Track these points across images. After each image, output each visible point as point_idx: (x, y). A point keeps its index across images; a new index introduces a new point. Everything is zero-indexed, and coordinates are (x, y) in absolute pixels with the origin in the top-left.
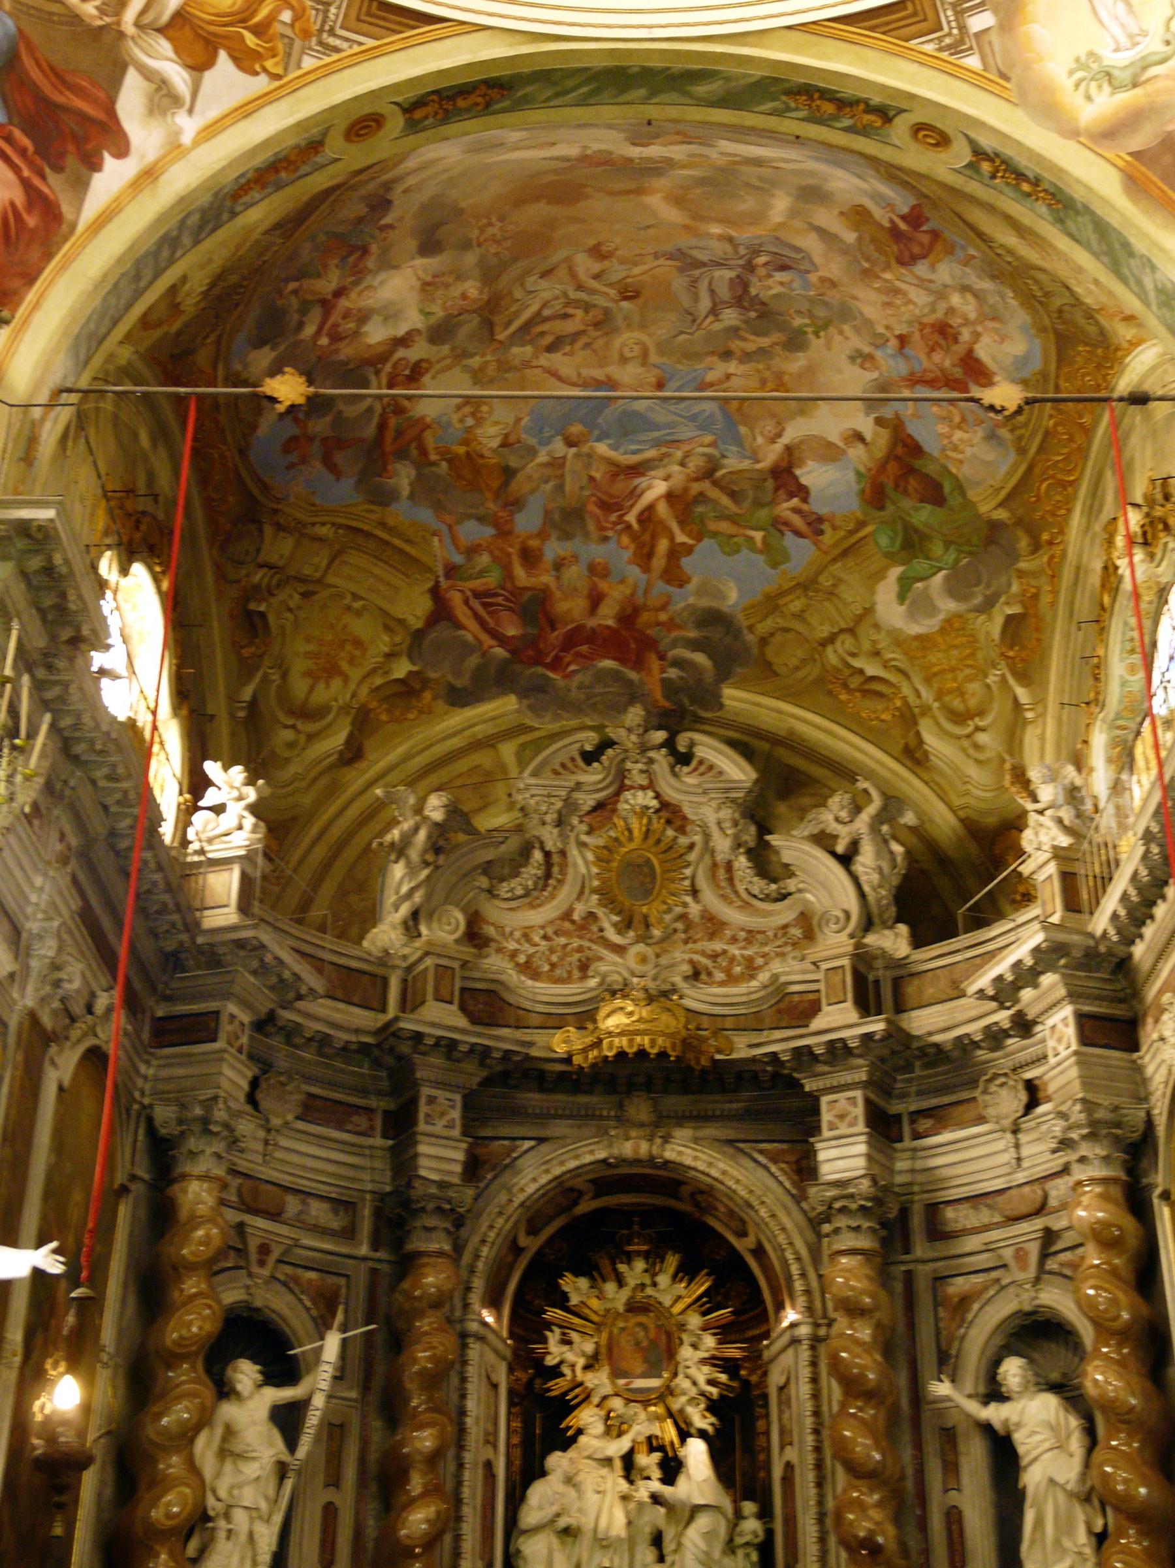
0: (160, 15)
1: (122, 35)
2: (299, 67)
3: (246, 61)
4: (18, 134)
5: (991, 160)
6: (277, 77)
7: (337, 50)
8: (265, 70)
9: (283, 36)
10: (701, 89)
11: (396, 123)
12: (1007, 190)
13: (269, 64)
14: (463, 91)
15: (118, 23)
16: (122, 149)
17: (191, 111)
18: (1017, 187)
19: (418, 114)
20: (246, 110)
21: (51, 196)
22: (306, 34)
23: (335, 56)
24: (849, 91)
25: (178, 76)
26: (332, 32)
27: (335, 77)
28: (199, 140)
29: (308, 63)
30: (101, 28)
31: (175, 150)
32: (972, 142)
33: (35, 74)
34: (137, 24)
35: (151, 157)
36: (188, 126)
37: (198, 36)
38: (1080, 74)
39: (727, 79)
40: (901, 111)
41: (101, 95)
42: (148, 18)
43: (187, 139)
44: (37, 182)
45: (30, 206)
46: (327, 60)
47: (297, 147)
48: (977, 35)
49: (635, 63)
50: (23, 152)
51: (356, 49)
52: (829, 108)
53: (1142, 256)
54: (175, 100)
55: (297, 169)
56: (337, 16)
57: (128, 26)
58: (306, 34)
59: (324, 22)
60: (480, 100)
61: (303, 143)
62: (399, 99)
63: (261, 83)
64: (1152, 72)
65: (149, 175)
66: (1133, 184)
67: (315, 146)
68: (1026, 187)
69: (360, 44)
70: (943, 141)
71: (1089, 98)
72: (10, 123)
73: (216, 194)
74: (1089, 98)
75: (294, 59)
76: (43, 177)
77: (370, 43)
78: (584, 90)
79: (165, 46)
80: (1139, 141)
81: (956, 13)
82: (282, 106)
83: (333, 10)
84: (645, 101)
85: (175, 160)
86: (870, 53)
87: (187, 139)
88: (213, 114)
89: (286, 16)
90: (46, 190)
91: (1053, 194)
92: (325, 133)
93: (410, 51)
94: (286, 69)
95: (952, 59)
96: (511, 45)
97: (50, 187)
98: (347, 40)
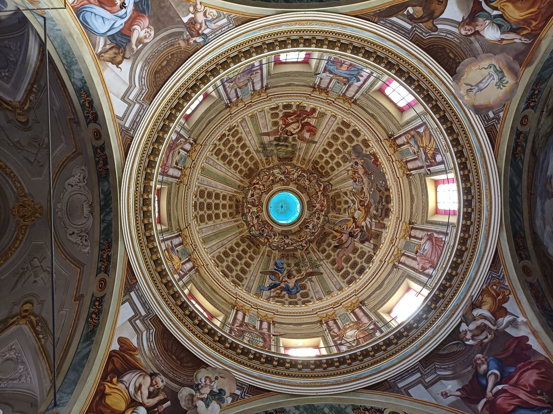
0: (493, 319)
1: (497, 330)
2: (508, 286)
3: (505, 300)
4: (519, 366)
5: (530, 103)
6: (510, 292)
7: (504, 276)
8: (508, 295)
9: (499, 289)
10: (516, 182)
11: (526, 262)
12: (539, 97)
13: (507, 294)
14: (516, 244)
15: (494, 330)
16: (526, 338)
17: (518, 317)
18: (537, 94)
19: (524, 256)
20: (519, 303)
21: (537, 362)
22: (499, 283)
23: (505, 276)
24: (513, 144)
25: (508, 318)
26: (499, 276)
27: (511, 277)
28: (526, 317)
29: (507, 284)
30: (494, 335)
31: (528, 324)
32: (524, 110)
33: (504, 356)
34: (494, 326)
35: (529, 331)
36: (521, 319)
37: (498, 311)
38: (501, 86)
39: (512, 176)
40: (517, 130)
41: (511, 340)
42: (493, 323)
43: (525, 320)
44: (533, 364)
45: (540, 369)
46: (506, 279)
47: (531, 290)
48: (494, 114)
49: (508, 199)
50: (524, 366)
51: (503, 271)
52: (519, 149)
53: (550, 54)
54: (514, 320)
55: (539, 291)
56: (495, 274)
57: (495, 328)
58: (499, 283)
59: (497, 278)
60: (520, 240)
61: (530, 288)
62: (518, 261)
63: (511, 296)
64: (498, 68)
65: (534, 333)
66: (529, 64)
67: (531, 285)
68: (536, 92)
69: (502, 270)
70: (526, 117)
71: (507, 82)
72: (514, 366)
73: (543, 315)
74: (507, 82)
75: (506, 287)
76: (532, 362)
77: (502, 267)
78: (517, 212)
79: (500, 320)
80: (517, 66)
81: (490, 121)
82: (517, 292)
83: (494, 275)
84: (521, 196)
85: (530, 324)
86: (501, 140)
87: (525, 320)
88: (519, 311)
89: (495, 287)
90: (535, 363)
91: (537, 84)
92: (527, 282)
93: (504, 257)
94: (508, 290)
95: (501, 120)
96: (503, 231)
97: (535, 362)
98: (501, 273)
